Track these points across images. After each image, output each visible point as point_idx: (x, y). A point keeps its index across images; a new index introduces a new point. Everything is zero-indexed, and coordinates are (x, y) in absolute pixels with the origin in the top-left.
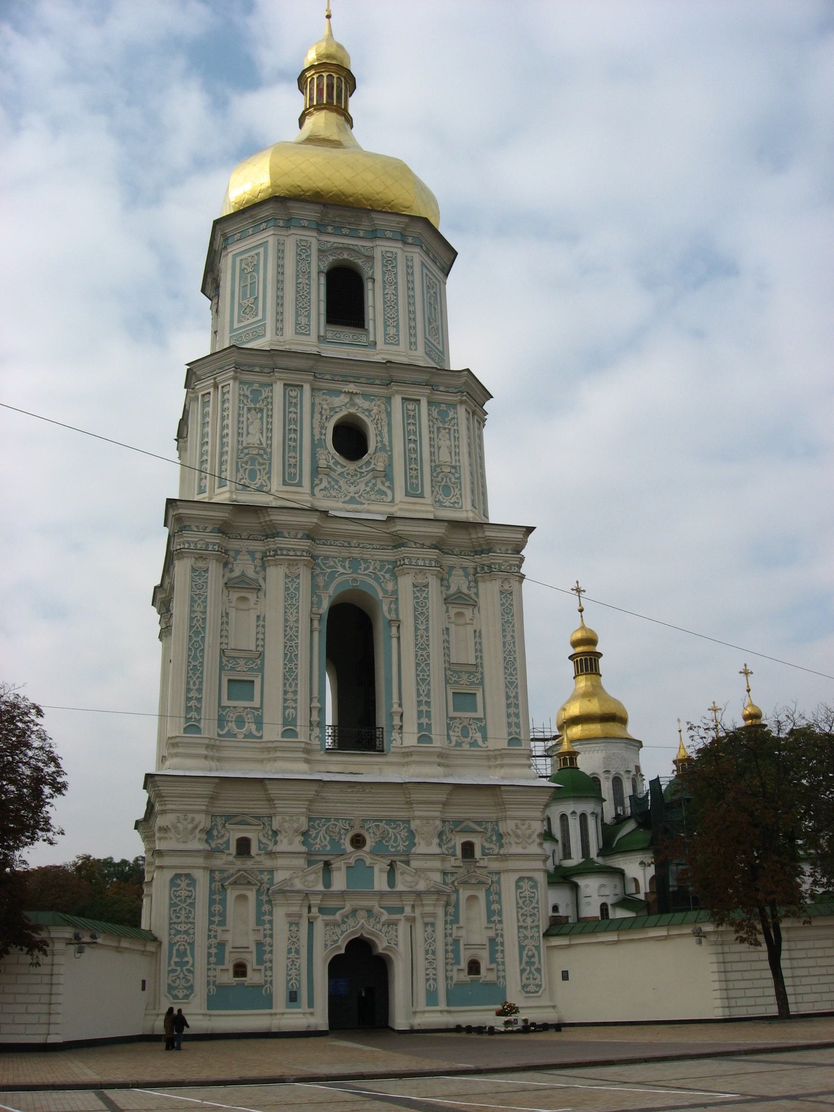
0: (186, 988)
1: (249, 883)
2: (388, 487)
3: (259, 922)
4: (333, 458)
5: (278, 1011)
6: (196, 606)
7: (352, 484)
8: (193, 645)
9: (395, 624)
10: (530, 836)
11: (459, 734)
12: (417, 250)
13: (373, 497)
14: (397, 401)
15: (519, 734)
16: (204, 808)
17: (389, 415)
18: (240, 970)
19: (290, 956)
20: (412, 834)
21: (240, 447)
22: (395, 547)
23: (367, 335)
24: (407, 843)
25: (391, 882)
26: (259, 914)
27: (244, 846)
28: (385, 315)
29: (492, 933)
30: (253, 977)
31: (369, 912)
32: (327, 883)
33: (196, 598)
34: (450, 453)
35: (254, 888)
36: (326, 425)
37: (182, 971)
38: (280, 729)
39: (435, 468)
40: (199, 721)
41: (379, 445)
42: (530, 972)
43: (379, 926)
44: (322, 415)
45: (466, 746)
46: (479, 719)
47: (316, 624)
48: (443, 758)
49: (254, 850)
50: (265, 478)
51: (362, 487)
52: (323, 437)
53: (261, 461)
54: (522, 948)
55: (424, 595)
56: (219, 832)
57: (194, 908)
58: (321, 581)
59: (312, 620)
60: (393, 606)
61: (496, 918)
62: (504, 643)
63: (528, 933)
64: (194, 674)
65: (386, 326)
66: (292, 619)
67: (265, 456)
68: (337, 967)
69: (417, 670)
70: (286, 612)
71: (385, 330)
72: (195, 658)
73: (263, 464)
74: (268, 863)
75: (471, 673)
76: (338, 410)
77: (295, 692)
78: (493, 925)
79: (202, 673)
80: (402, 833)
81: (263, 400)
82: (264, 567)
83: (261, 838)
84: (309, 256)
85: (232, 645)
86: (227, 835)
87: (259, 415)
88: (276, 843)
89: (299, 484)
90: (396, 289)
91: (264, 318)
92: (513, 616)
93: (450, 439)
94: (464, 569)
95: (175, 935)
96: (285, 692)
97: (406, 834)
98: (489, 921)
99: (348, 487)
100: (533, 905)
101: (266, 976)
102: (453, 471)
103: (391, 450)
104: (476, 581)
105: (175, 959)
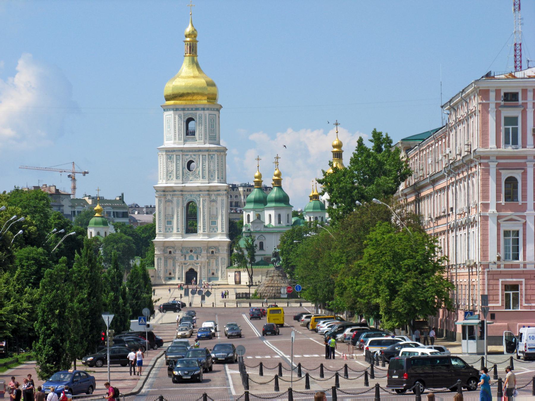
3: (173, 266)
14: (201, 157)
18: (170, 274)
25: (197, 259)
27: (170, 252)
30: (172, 275)
32: (185, 259)
39: (209, 171)
58: (184, 199)
68: (187, 273)
74: (175, 255)
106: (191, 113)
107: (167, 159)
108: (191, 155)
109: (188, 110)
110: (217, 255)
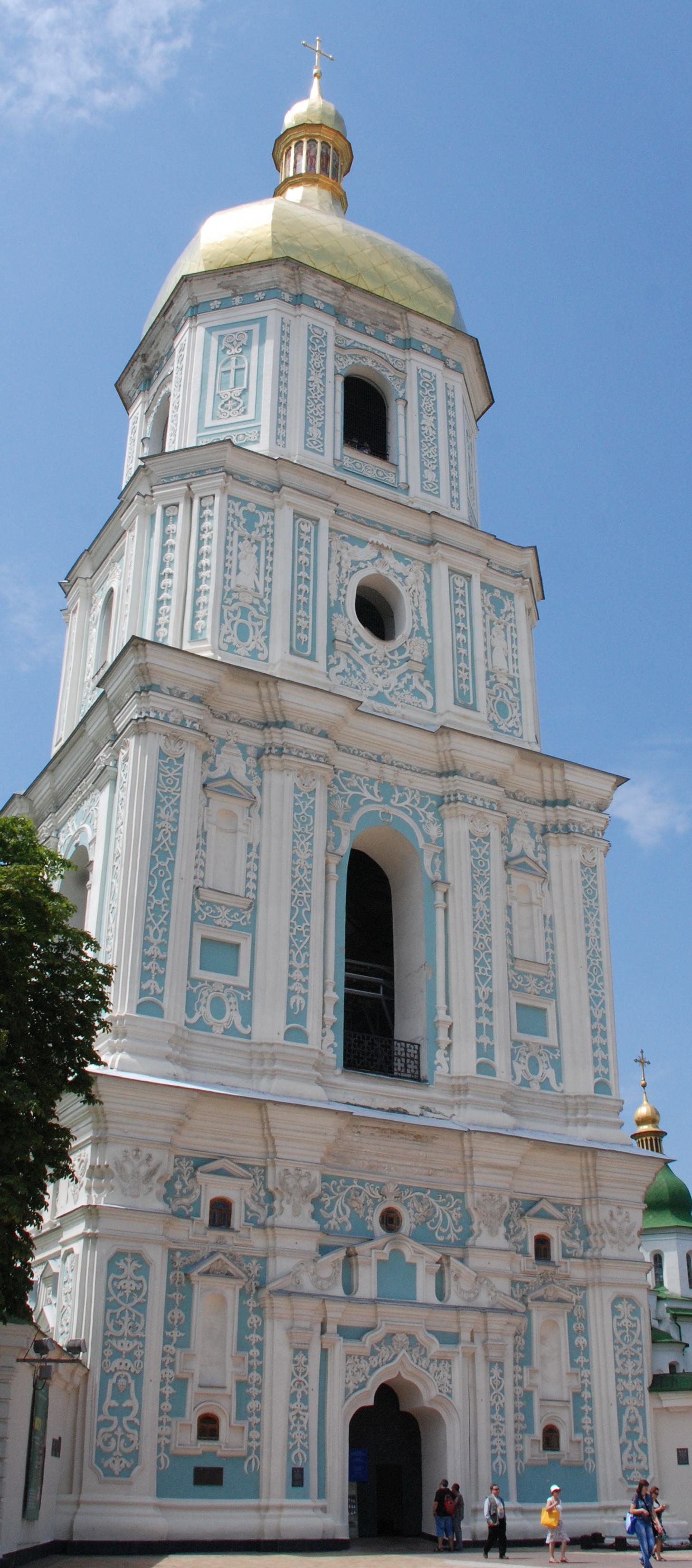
0: (126, 1455)
1: (229, 1275)
2: (428, 688)
3: (242, 1345)
4: (355, 631)
5: (273, 1502)
6: (163, 810)
7: (381, 673)
8: (156, 871)
9: (442, 888)
10: (629, 1233)
11: (526, 1067)
12: (459, 378)
13: (408, 698)
14: (441, 572)
15: (607, 1076)
16: (168, 1140)
17: (428, 588)
18: (208, 1427)
19: (294, 1406)
20: (467, 1219)
21: (228, 589)
22: (440, 775)
23: (397, 474)
24: (460, 1230)
25: (440, 1293)
26: (243, 1330)
28: (421, 453)
29: (576, 1383)
31: (412, 1339)
32: (349, 1287)
33: (164, 799)
34: (507, 658)
35: (239, 1284)
36: (346, 582)
37: (120, 1423)
38: (282, 1025)
40: (161, 996)
41: (417, 628)
42: (633, 1449)
43: (424, 1362)
44: (340, 569)
45: (536, 1087)
46: (552, 1049)
47: (333, 869)
48: (509, 1102)
49: (237, 1218)
50: (262, 640)
51: (392, 680)
52: (342, 599)
53: (256, 615)
54: (621, 1409)
55: (484, 851)
56: (184, 1186)
57: (144, 1312)
59: (327, 864)
60: (438, 861)
61: (581, 1359)
62: (587, 939)
63: (629, 1385)
64: (156, 919)
65: (423, 468)
66: (303, 855)
67: (261, 609)
69: (475, 961)
70: (294, 844)
71: (422, 473)
72: (158, 893)
73: (259, 620)
75: (540, 978)
76: (362, 565)
77: (305, 971)
78: (577, 1370)
79: (168, 918)
80: (454, 1213)
81: (260, 529)
82: (260, 772)
83: (249, 1201)
84: (325, 349)
85: (209, 883)
86: (197, 1191)
87: (255, 548)
88: (271, 1211)
89: (312, 657)
90: (435, 421)
91: (257, 417)
92: (596, 901)
93: (506, 639)
94: (530, 825)
95: (112, 1358)
96: (291, 969)
97: (459, 1215)
98: (573, 1364)
99: (374, 677)
100: (634, 1342)
101: (250, 1440)
102: (511, 683)
103: (432, 637)
104: (545, 845)
105: (109, 1402)
106: (372, 352)
107: (230, 520)
108: (380, 547)
109: (360, 328)
110: (578, 1272)
